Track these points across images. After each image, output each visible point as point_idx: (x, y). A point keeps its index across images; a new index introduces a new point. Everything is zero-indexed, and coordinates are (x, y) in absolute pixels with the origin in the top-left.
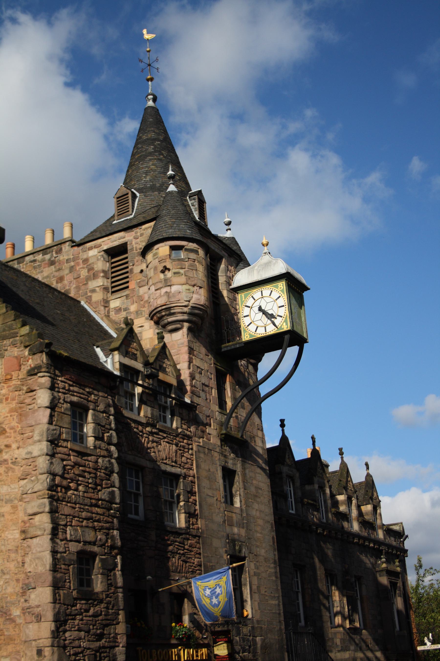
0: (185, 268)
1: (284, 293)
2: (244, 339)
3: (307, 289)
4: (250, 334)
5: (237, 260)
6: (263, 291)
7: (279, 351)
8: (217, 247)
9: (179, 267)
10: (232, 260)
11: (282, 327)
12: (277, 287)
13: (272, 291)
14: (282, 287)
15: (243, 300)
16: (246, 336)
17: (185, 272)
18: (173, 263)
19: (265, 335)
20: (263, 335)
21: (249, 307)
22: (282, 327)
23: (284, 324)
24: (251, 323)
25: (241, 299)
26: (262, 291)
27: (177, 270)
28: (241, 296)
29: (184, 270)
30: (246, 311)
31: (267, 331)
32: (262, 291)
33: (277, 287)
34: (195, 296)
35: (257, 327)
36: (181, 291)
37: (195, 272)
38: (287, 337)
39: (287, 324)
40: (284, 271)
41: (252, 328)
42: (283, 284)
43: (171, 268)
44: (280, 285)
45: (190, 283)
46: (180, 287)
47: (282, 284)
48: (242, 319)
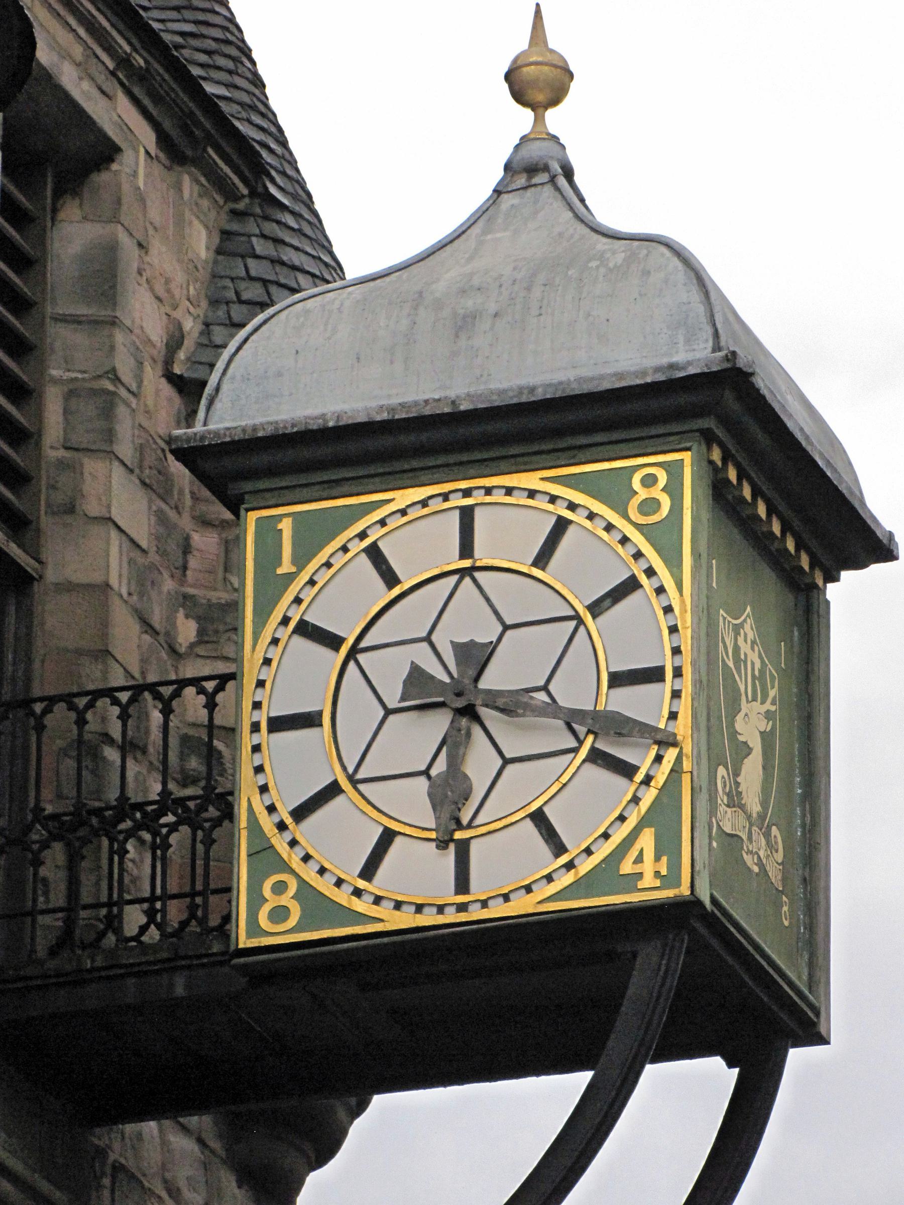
1: (673, 562)
2: (254, 929)
3: (879, 549)
4: (306, 891)
5: (230, 195)
6: (480, 518)
7: (567, 1089)
8: (78, 51)
10: (186, 180)
11: (627, 867)
12: (615, 492)
15: (286, 567)
16: (272, 902)
19: (451, 917)
21: (332, 641)
22: (627, 867)
23: (647, 841)
24: (332, 790)
25: (269, 555)
26: (467, 514)
30: (296, 676)
31: (478, 888)
32: (467, 515)
35: (387, 838)
38: (650, 974)
39: (667, 846)
40: (695, 355)
41: (338, 838)
42: (674, 470)
44: (649, 481)
47: (662, 478)
48: (247, 740)
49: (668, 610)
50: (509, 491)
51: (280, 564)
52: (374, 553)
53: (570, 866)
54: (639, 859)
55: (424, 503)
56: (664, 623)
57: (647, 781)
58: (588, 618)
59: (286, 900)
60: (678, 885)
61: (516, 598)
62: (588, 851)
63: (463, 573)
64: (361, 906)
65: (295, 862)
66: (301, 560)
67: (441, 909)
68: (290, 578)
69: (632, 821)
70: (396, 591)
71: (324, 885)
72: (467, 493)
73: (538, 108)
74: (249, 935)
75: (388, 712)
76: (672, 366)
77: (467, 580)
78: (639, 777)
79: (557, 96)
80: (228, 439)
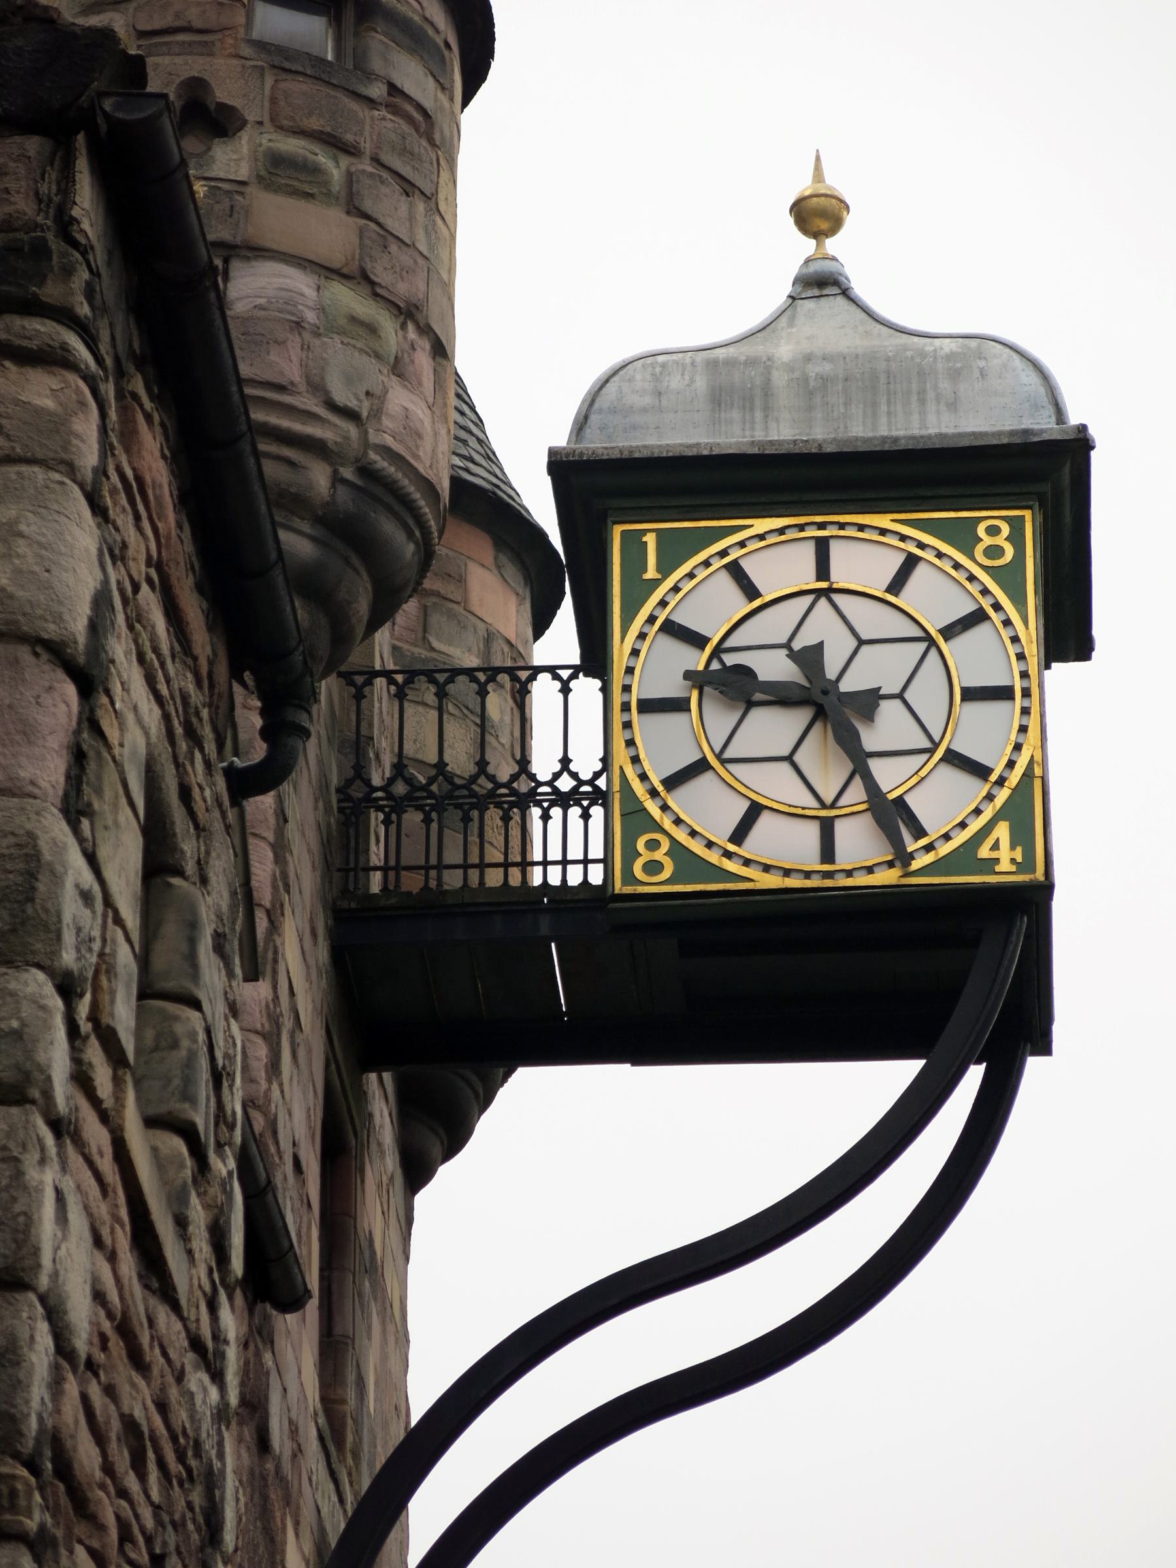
0: (351, 151)
1: (1019, 600)
2: (629, 877)
9: (314, 124)
11: (984, 852)
12: (963, 536)
13: (911, 562)
15: (651, 573)
16: (646, 856)
17: (350, 178)
18: (269, 81)
22: (984, 852)
23: (1002, 831)
27: (293, 146)
28: (634, 543)
29: (345, 161)
34: (399, 398)
35: (754, 811)
36: (311, 316)
37: (421, 207)
43: (251, 117)
45: (382, 275)
46: (301, 283)
47: (1006, 529)
49: (1015, 639)
50: (861, 527)
51: (646, 571)
52: (736, 571)
53: (929, 848)
54: (996, 846)
55: (781, 531)
56: (1012, 650)
57: (1001, 782)
58: (940, 640)
59: (659, 855)
60: (1034, 871)
61: (871, 619)
62: (947, 837)
63: (819, 593)
64: (731, 866)
65: (667, 824)
66: (665, 569)
67: (808, 875)
68: (656, 583)
69: (988, 814)
70: (757, 603)
71: (696, 847)
72: (822, 526)
73: (818, 235)
74: (624, 883)
76: (1026, 432)
77: (823, 602)
78: (993, 777)
79: (836, 224)
80: (605, 457)
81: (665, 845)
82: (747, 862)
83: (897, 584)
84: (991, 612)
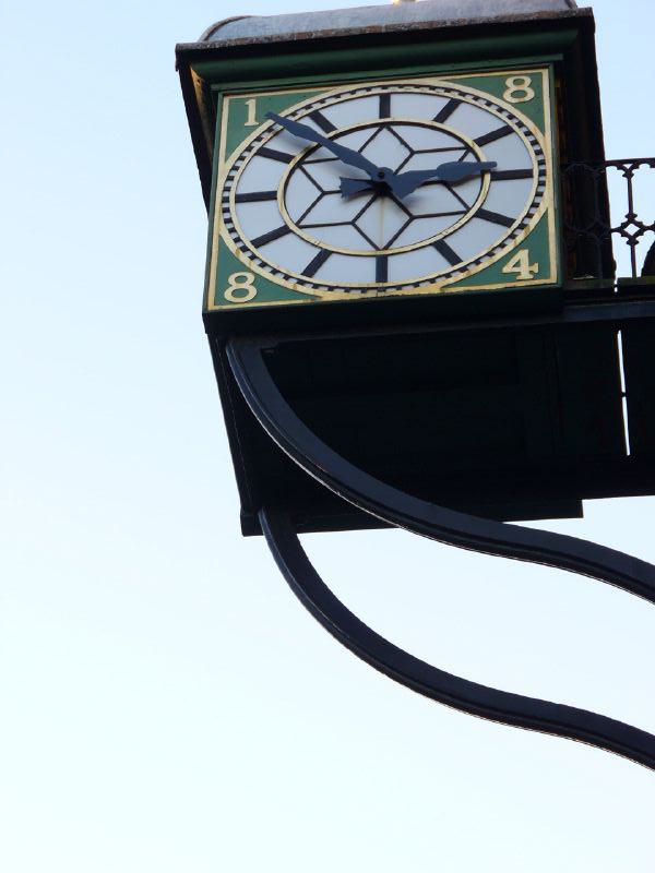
11: (507, 269)
14: (531, 94)
15: (251, 121)
19: (371, 294)
20: (356, 295)
22: (507, 269)
23: (523, 255)
33: (499, 90)
35: (324, 255)
39: (538, 256)
47: (528, 81)
51: (247, 120)
54: (517, 264)
60: (548, 277)
63: (381, 126)
68: (254, 128)
69: (510, 246)
71: (278, 280)
72: (384, 87)
75: (324, 193)
77: (385, 131)
81: (251, 278)
82: (316, 286)
83: (443, 116)
84: (515, 128)
